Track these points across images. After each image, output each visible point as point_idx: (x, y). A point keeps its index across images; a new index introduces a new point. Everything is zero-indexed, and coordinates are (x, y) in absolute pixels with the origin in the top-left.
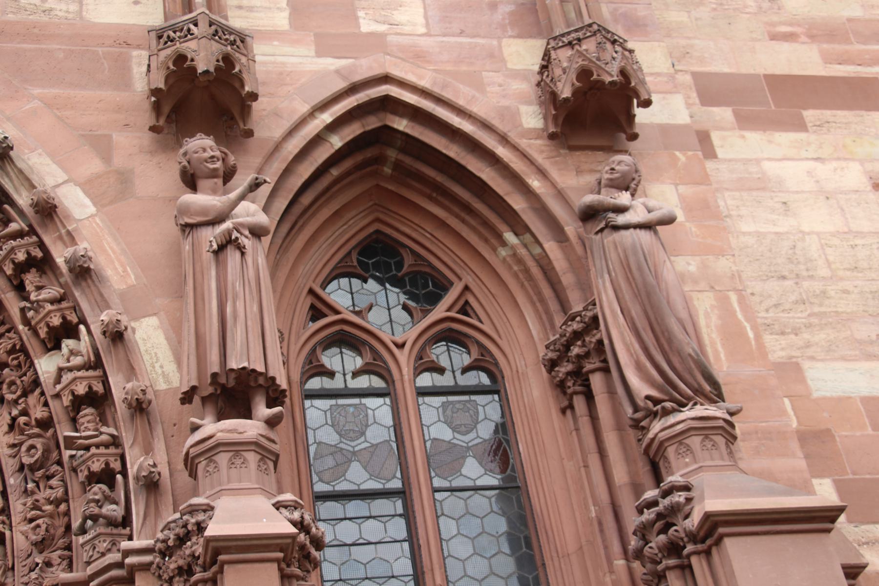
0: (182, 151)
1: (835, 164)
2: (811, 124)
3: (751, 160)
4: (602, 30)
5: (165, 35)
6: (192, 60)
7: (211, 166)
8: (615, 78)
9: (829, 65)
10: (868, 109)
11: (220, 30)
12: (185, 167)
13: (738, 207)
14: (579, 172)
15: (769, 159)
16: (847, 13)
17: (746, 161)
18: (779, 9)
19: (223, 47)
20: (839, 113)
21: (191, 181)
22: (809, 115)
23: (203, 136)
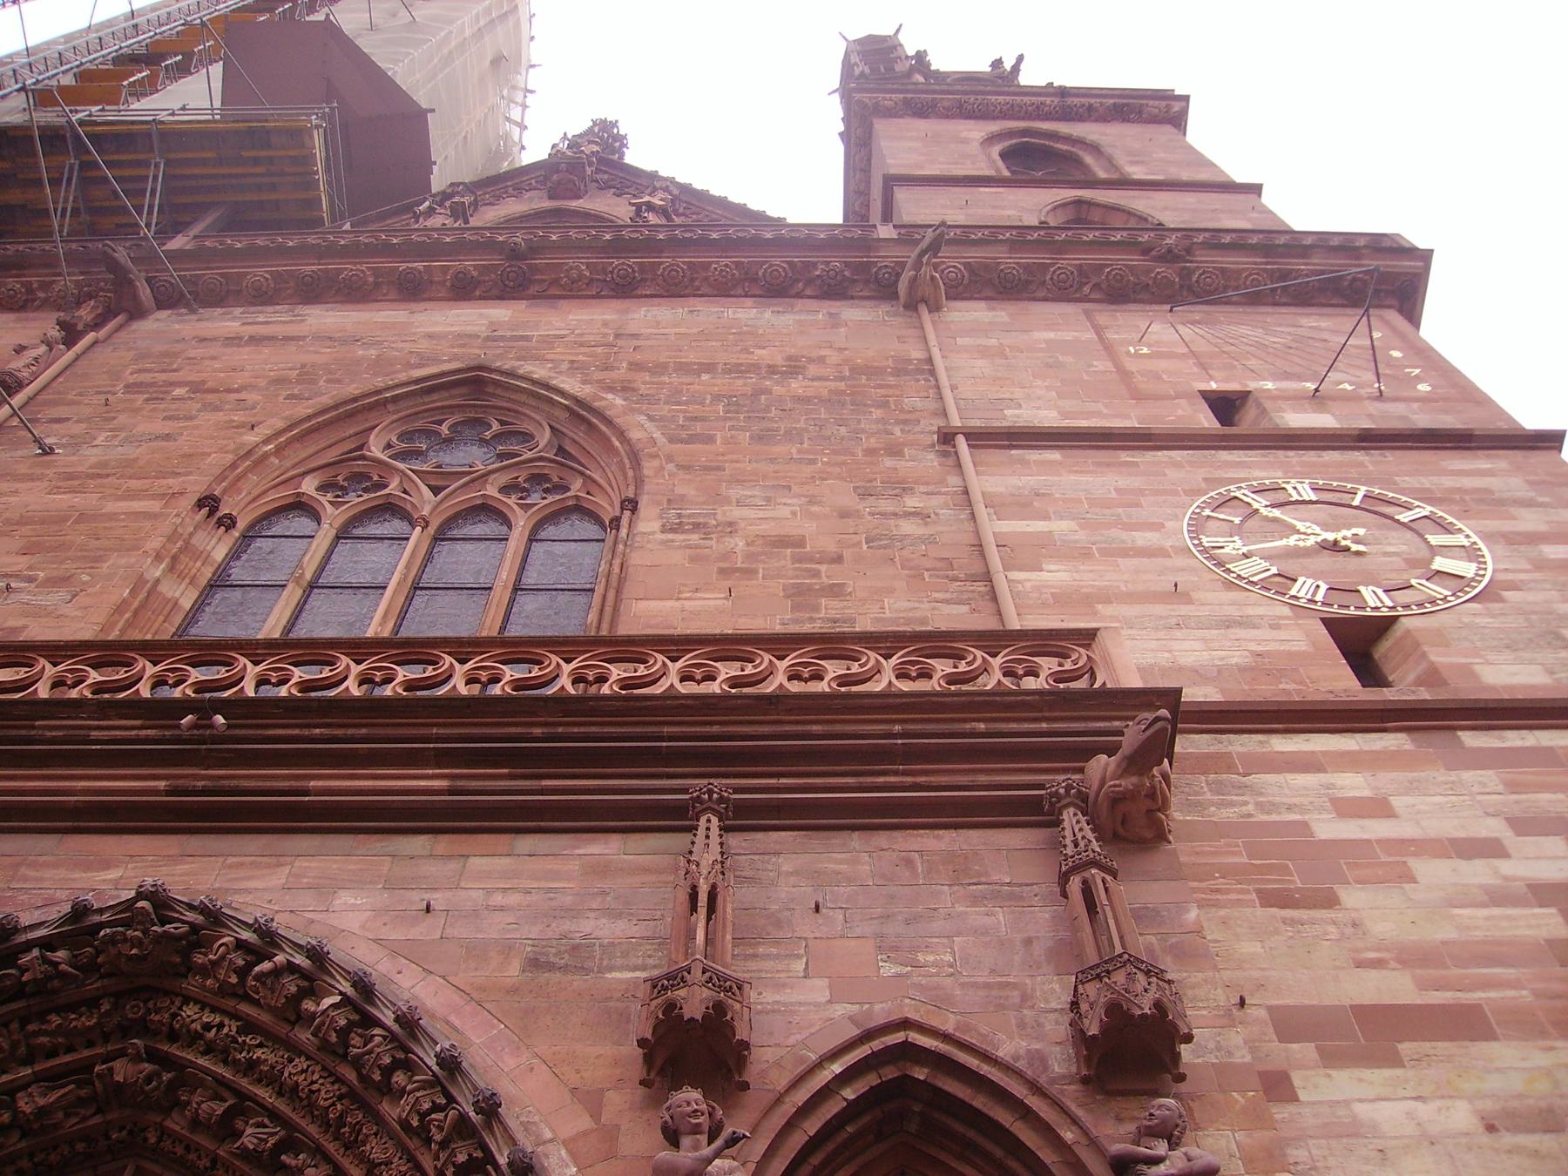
0: (667, 1104)
1: (1439, 1103)
2: (1408, 1058)
3: (1338, 1102)
4: (1135, 961)
5: (660, 984)
6: (681, 1008)
7: (694, 1121)
8: (1147, 1011)
9: (1424, 993)
10: (1473, 1040)
11: (715, 977)
12: (666, 1122)
13: (1324, 1157)
14: (1119, 1119)
15: (1361, 1100)
16: (1440, 936)
17: (1333, 1104)
18: (1364, 934)
19: (714, 993)
20: (1440, 1044)
21: (672, 1137)
22: (1405, 1048)
23: (690, 1089)
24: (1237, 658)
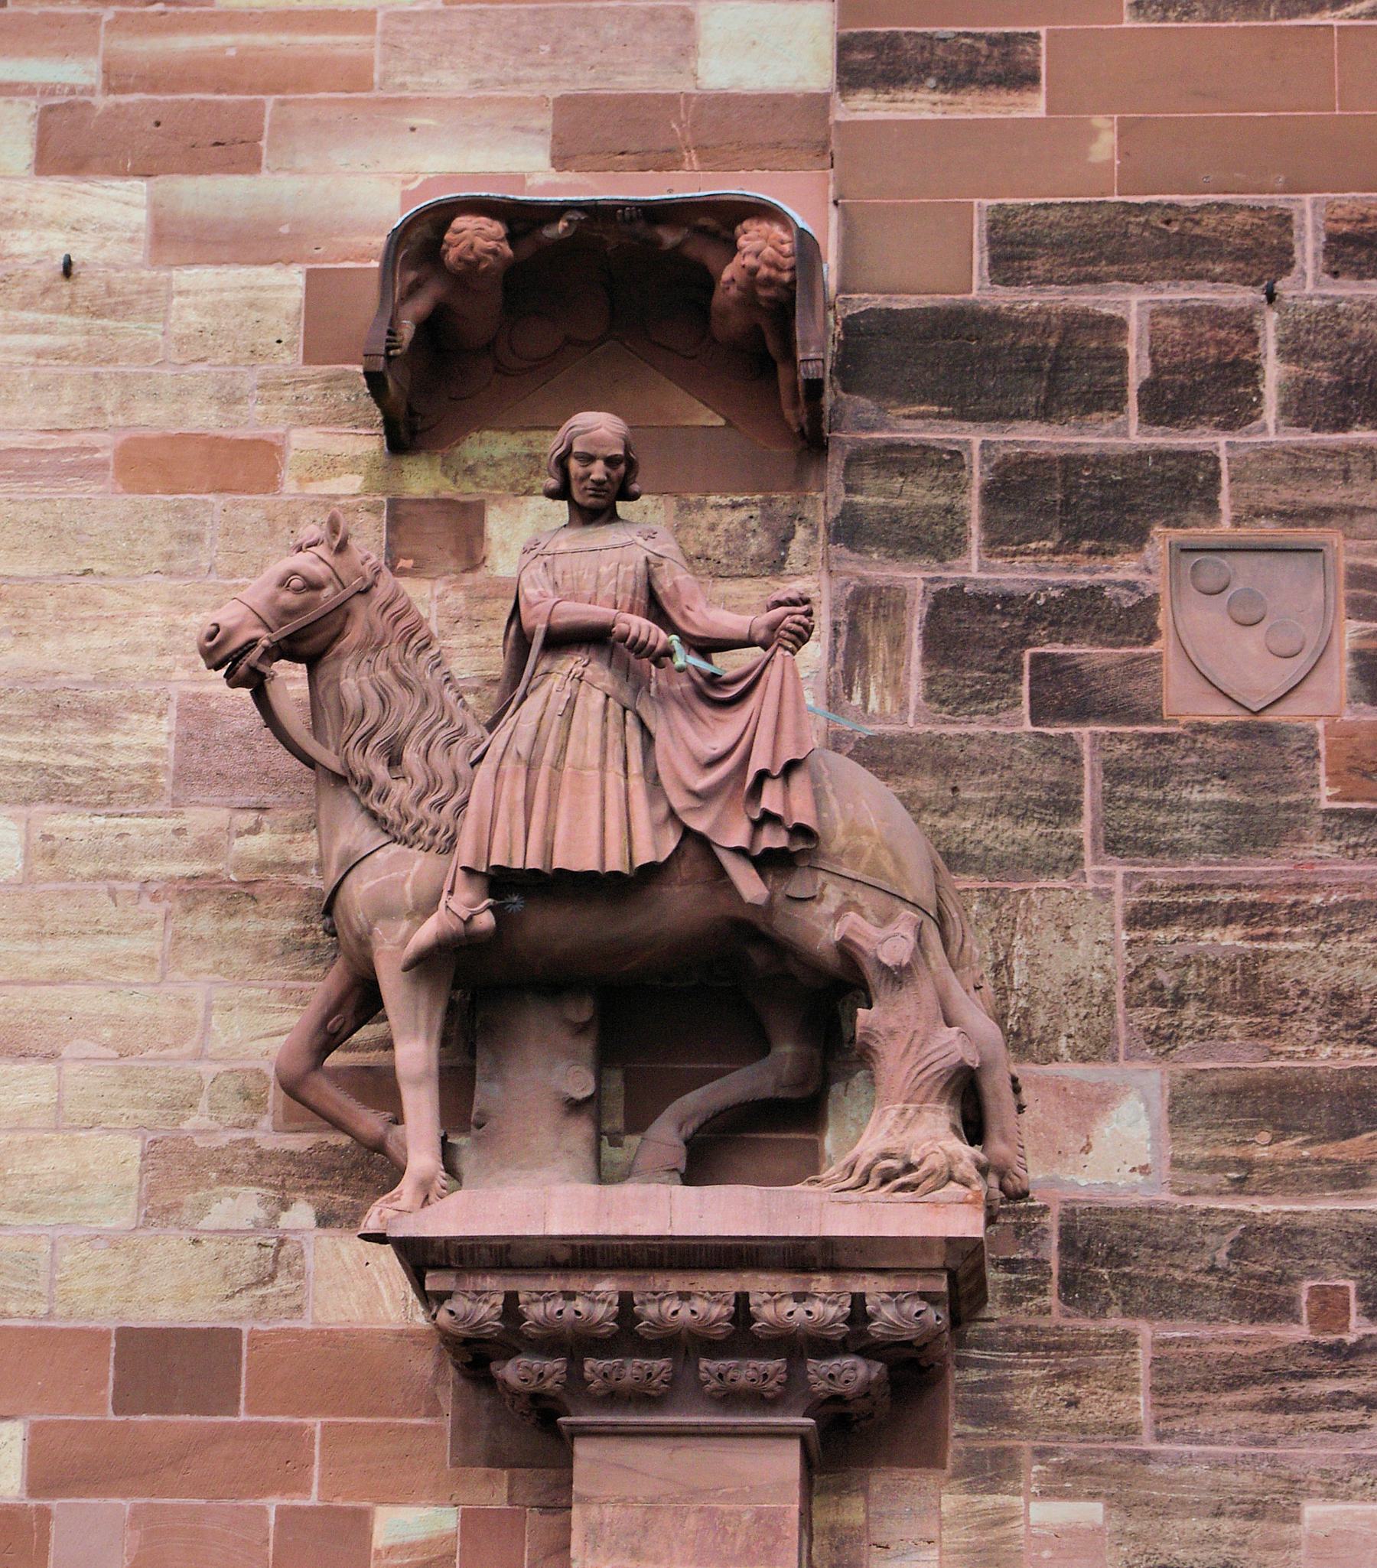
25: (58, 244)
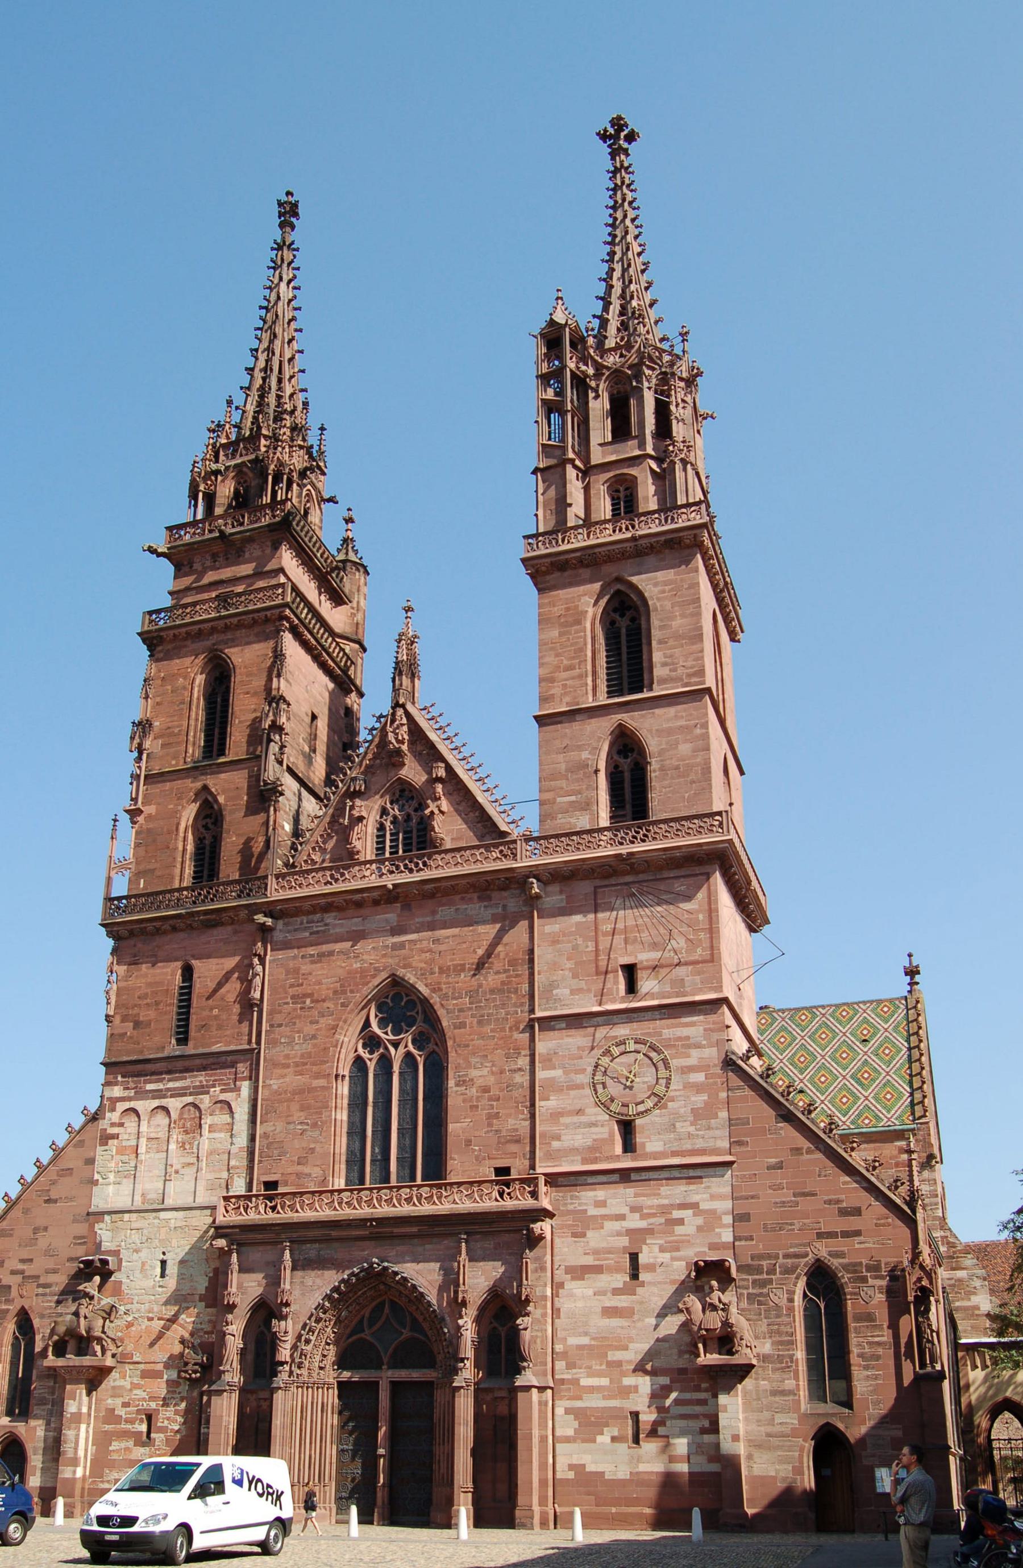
24: (589, 1142)
25: (662, 1260)
